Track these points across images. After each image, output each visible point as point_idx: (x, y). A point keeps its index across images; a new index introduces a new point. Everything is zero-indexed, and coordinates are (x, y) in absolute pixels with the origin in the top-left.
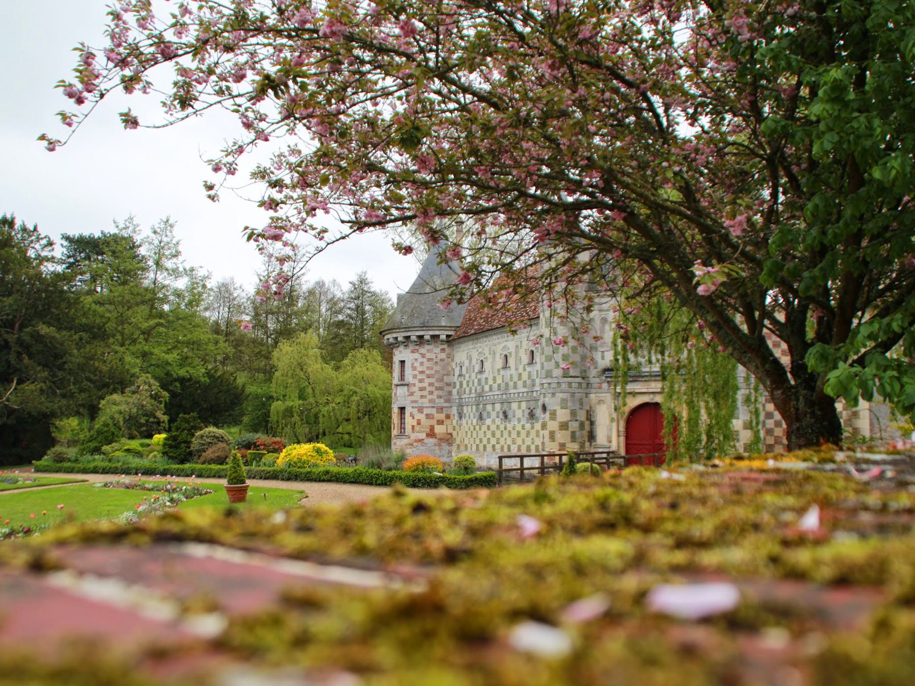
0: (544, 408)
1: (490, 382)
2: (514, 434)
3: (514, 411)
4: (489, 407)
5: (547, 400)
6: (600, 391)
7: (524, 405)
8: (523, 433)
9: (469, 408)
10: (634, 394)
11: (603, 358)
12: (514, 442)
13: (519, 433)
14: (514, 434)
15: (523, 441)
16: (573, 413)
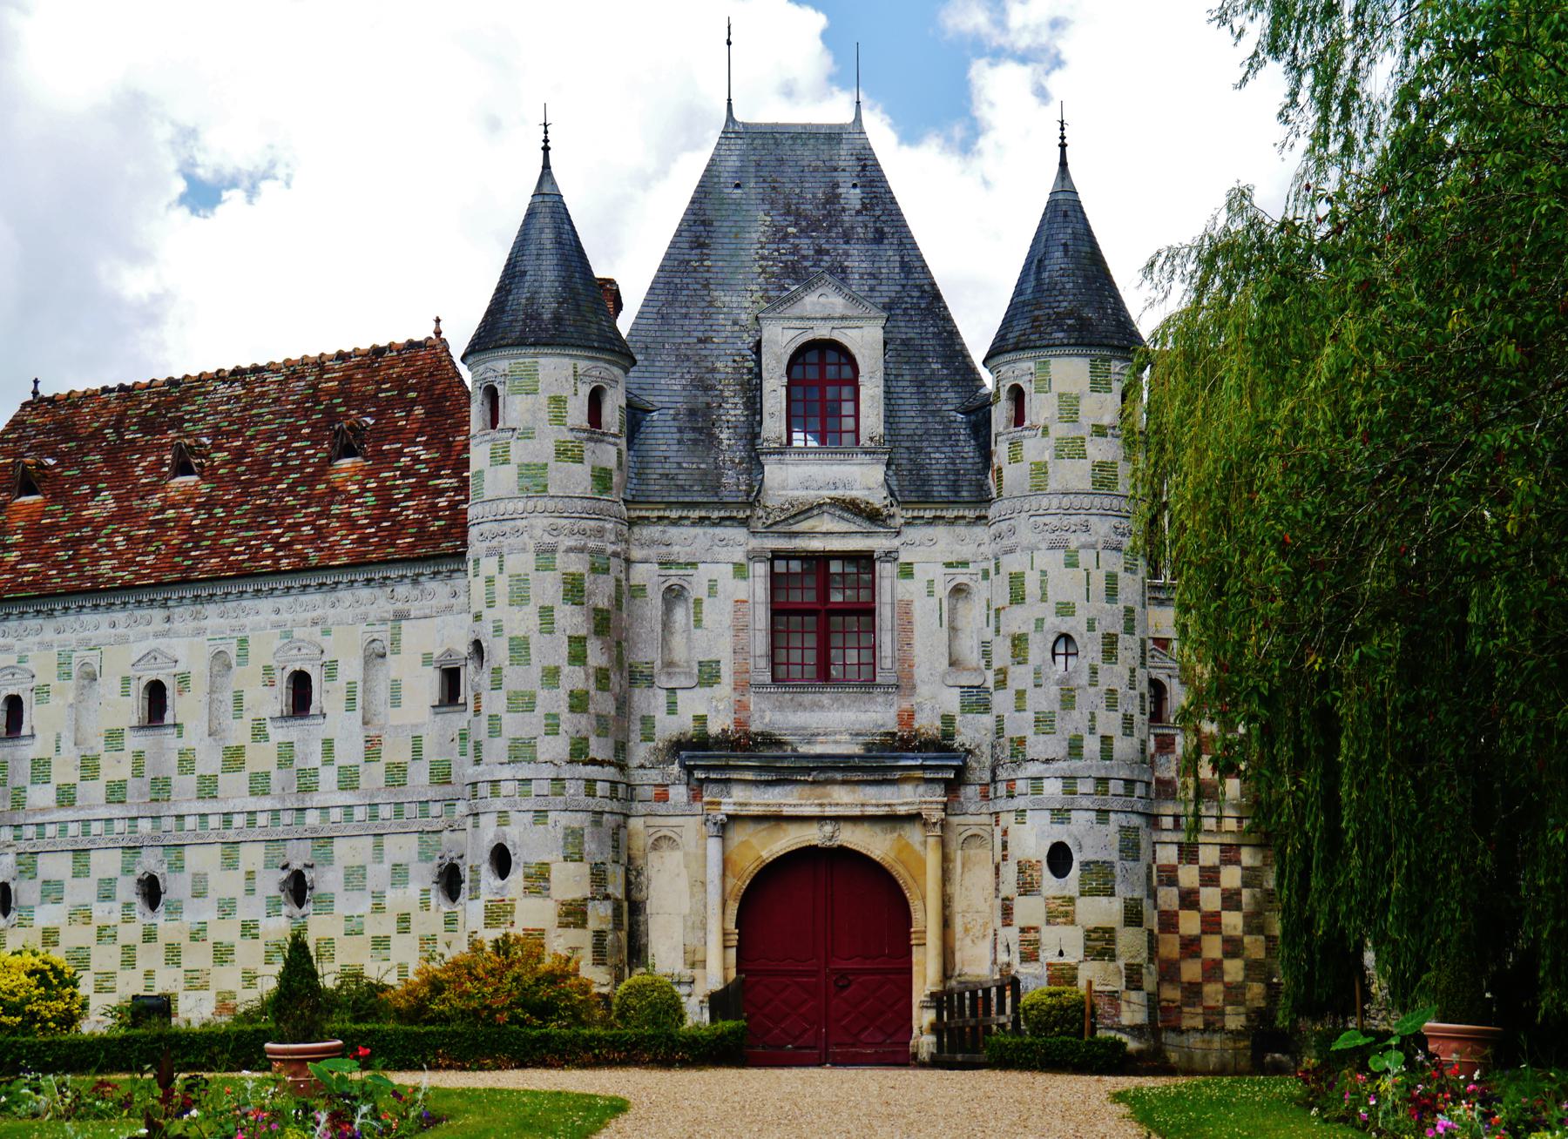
0: (501, 860)
1: (65, 771)
2: (198, 957)
4: (55, 866)
5: (517, 835)
6: (660, 808)
7: (253, 856)
10: (777, 819)
11: (672, 708)
14: (198, 957)
16: (598, 876)
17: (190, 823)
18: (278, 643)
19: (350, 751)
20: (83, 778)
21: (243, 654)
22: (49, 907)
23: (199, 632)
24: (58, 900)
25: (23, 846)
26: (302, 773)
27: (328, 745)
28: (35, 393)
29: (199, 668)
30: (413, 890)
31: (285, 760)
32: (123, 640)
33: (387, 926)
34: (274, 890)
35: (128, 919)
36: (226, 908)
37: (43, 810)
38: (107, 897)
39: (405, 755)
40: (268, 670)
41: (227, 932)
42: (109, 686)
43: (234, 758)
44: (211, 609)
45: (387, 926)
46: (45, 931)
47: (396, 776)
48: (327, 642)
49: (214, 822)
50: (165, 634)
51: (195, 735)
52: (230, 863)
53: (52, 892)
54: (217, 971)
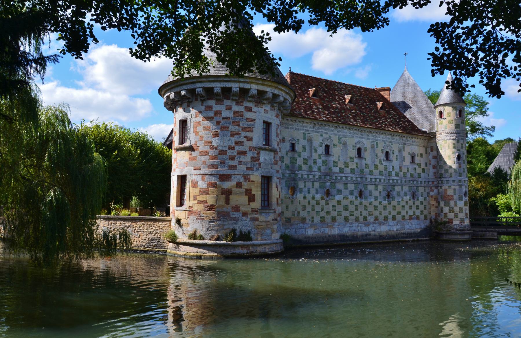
1: (341, 165)
2: (371, 208)
3: (371, 192)
7: (380, 188)
8: (380, 208)
9: (309, 184)
12: (370, 214)
13: (376, 208)
14: (371, 208)
15: (381, 213)
17: (369, 180)
18: (384, 145)
19: (397, 169)
20: (345, 167)
21: (377, 146)
22: (339, 196)
23: (368, 139)
24: (341, 194)
25: (333, 181)
26: (389, 172)
27: (393, 167)
28: (290, 70)
29: (369, 147)
30: (408, 197)
31: (386, 168)
32: (353, 137)
33: (404, 204)
34: (385, 196)
35: (356, 200)
36: (376, 198)
37: (337, 173)
38: (351, 193)
39: (406, 171)
40: (382, 150)
41: (376, 203)
42: (350, 147)
43: (376, 167)
44: (370, 135)
45: (404, 204)
46: (338, 201)
47: (405, 174)
48: (392, 146)
49: (373, 180)
50: (362, 138)
51: (369, 161)
52: (376, 189)
53: (339, 192)
54: (375, 211)
